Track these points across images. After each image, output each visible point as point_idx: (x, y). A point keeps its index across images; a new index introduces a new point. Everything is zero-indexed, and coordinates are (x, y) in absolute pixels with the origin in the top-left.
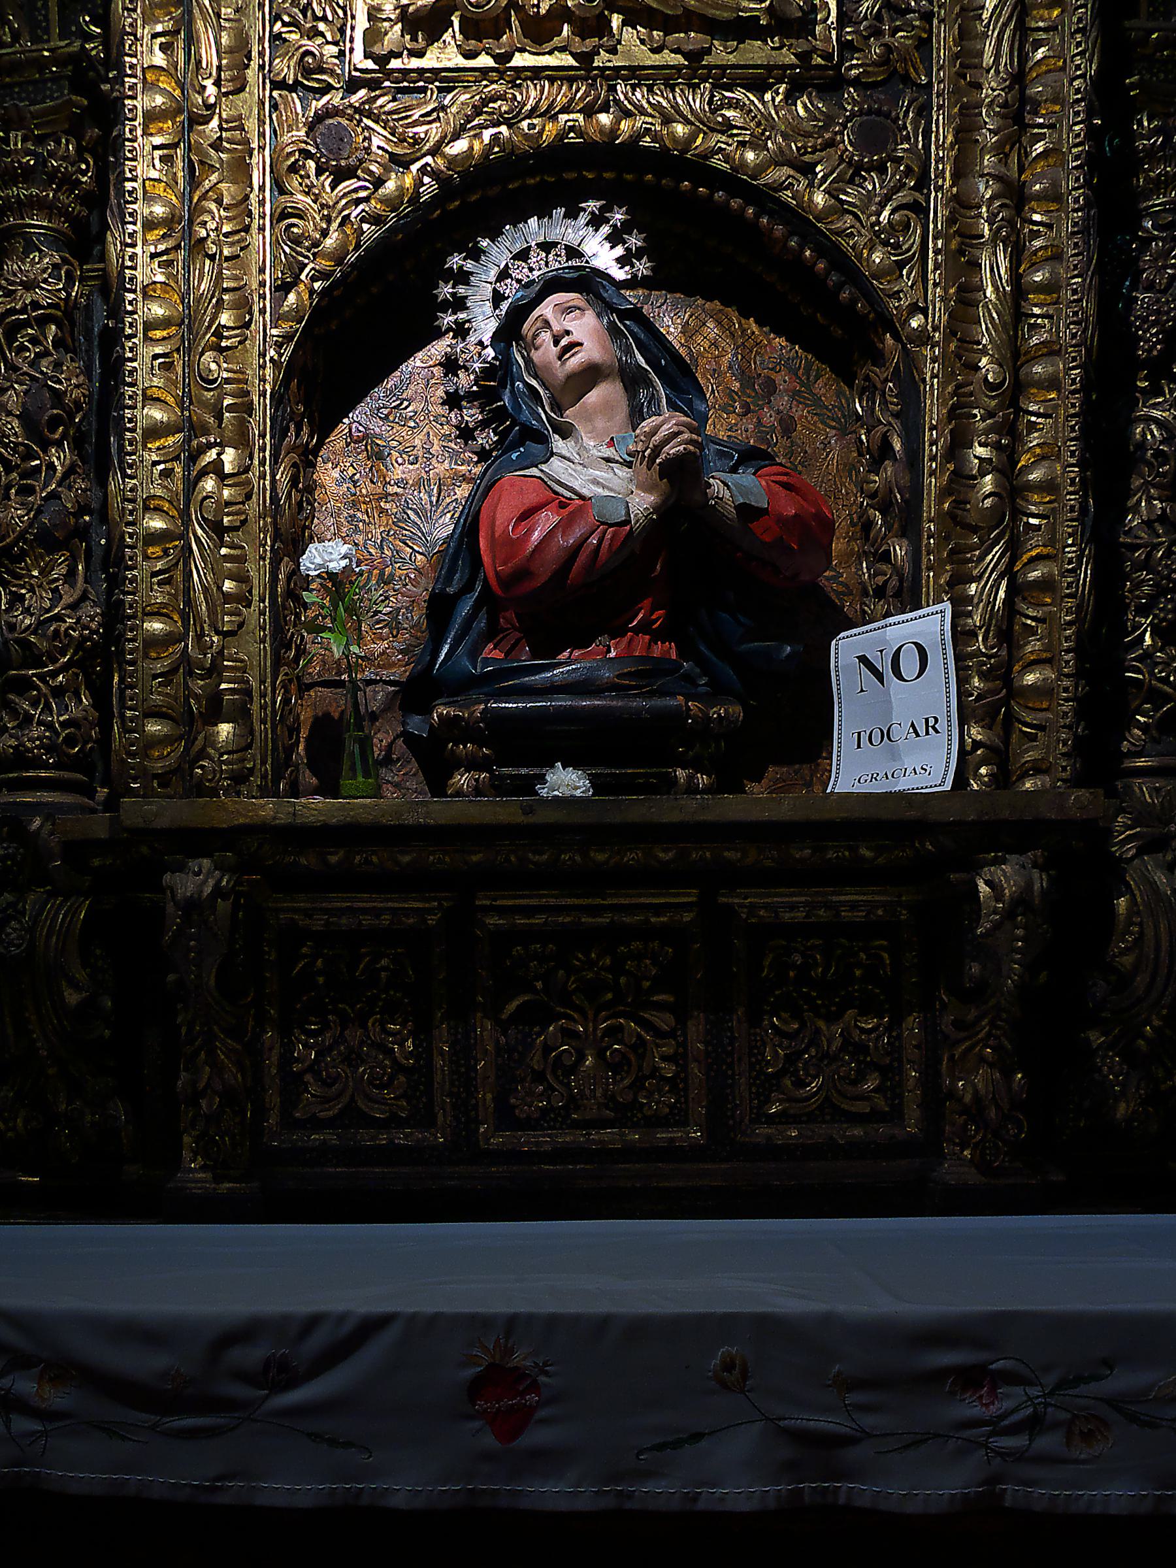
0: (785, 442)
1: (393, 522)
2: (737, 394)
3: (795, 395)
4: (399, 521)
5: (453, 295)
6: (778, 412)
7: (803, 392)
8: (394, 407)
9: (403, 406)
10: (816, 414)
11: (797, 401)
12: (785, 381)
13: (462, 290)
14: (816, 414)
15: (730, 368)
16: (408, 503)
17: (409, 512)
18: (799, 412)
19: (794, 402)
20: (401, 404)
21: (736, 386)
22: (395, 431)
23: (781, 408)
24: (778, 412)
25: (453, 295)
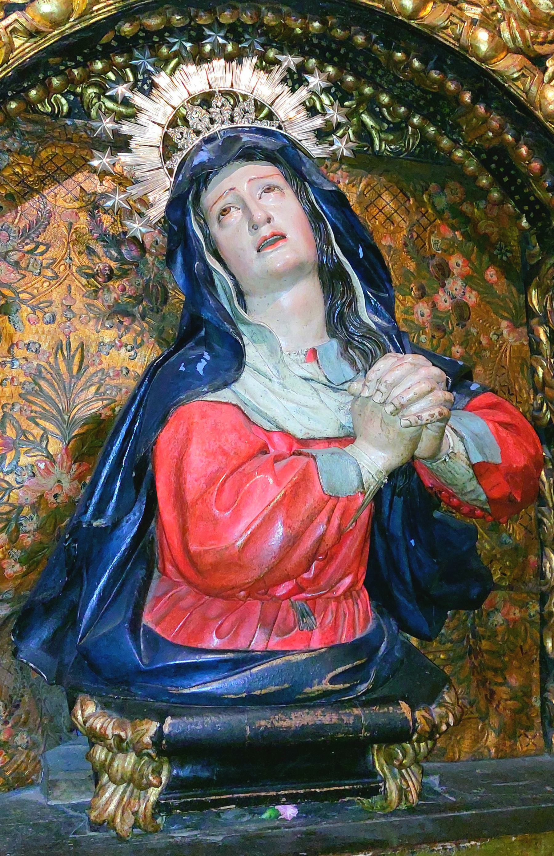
0: (458, 330)
1: (20, 395)
2: (412, 274)
3: (467, 280)
4: (29, 393)
5: (115, 132)
6: (453, 297)
7: (475, 277)
8: (29, 252)
9: (39, 251)
10: (488, 302)
11: (470, 287)
12: (458, 265)
13: (126, 128)
14: (488, 302)
15: (405, 245)
16: (40, 372)
17: (42, 383)
18: (472, 298)
19: (468, 289)
20: (36, 248)
21: (412, 266)
22: (27, 280)
23: (455, 292)
24: (453, 297)
25: (115, 132)
